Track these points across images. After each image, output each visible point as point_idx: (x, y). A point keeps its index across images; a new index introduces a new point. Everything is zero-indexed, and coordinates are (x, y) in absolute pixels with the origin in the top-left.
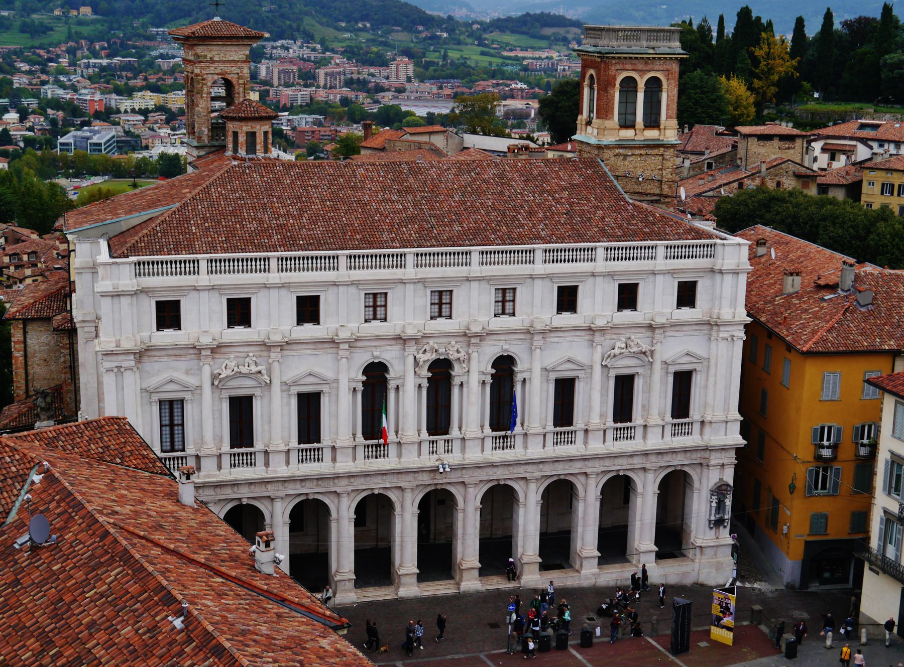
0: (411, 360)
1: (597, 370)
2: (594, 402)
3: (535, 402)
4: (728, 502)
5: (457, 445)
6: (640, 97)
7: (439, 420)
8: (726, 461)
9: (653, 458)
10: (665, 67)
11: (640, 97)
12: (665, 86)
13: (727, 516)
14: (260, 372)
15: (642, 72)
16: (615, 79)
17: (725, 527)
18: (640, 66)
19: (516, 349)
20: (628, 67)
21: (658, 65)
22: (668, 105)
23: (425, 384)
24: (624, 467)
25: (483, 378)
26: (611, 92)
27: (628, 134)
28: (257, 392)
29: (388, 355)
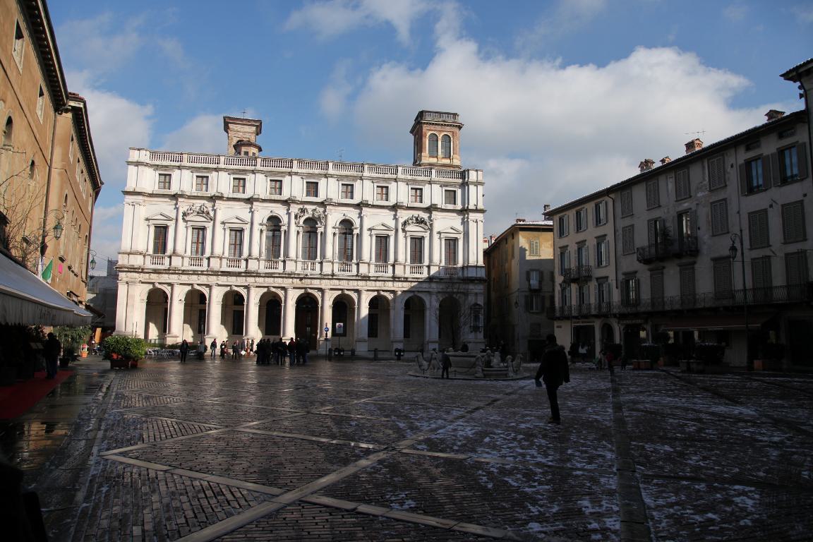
0: (293, 216)
1: (400, 231)
2: (401, 250)
4: (481, 317)
7: (311, 252)
13: (481, 324)
14: (208, 213)
17: (480, 332)
18: (439, 128)
19: (352, 214)
20: (432, 128)
23: (301, 230)
24: (417, 290)
25: (334, 230)
27: (434, 160)
29: (280, 211)
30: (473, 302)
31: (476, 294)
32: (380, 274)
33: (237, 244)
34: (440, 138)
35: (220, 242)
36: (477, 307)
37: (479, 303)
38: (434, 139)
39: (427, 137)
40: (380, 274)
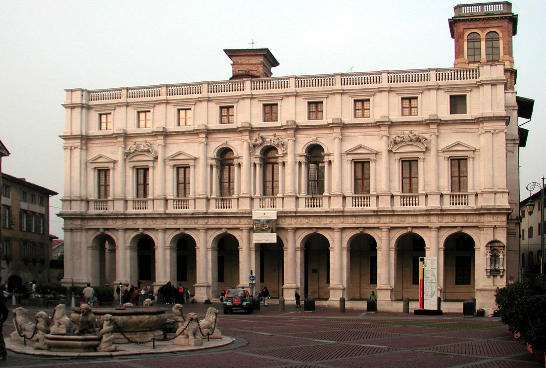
3: (339, 177)
5: (279, 202)
6: (483, 44)
7: (269, 188)
8: (497, 224)
9: (434, 219)
10: (499, 25)
11: (483, 44)
12: (501, 35)
15: (482, 29)
16: (463, 33)
21: (494, 23)
22: (504, 47)
24: (410, 225)
26: (461, 41)
28: (150, 164)
30: (491, 238)
31: (495, 227)
32: (360, 208)
33: (182, 185)
34: (483, 35)
35: (162, 182)
36: (497, 244)
37: (499, 239)
38: (474, 40)
39: (465, 37)
40: (360, 208)
